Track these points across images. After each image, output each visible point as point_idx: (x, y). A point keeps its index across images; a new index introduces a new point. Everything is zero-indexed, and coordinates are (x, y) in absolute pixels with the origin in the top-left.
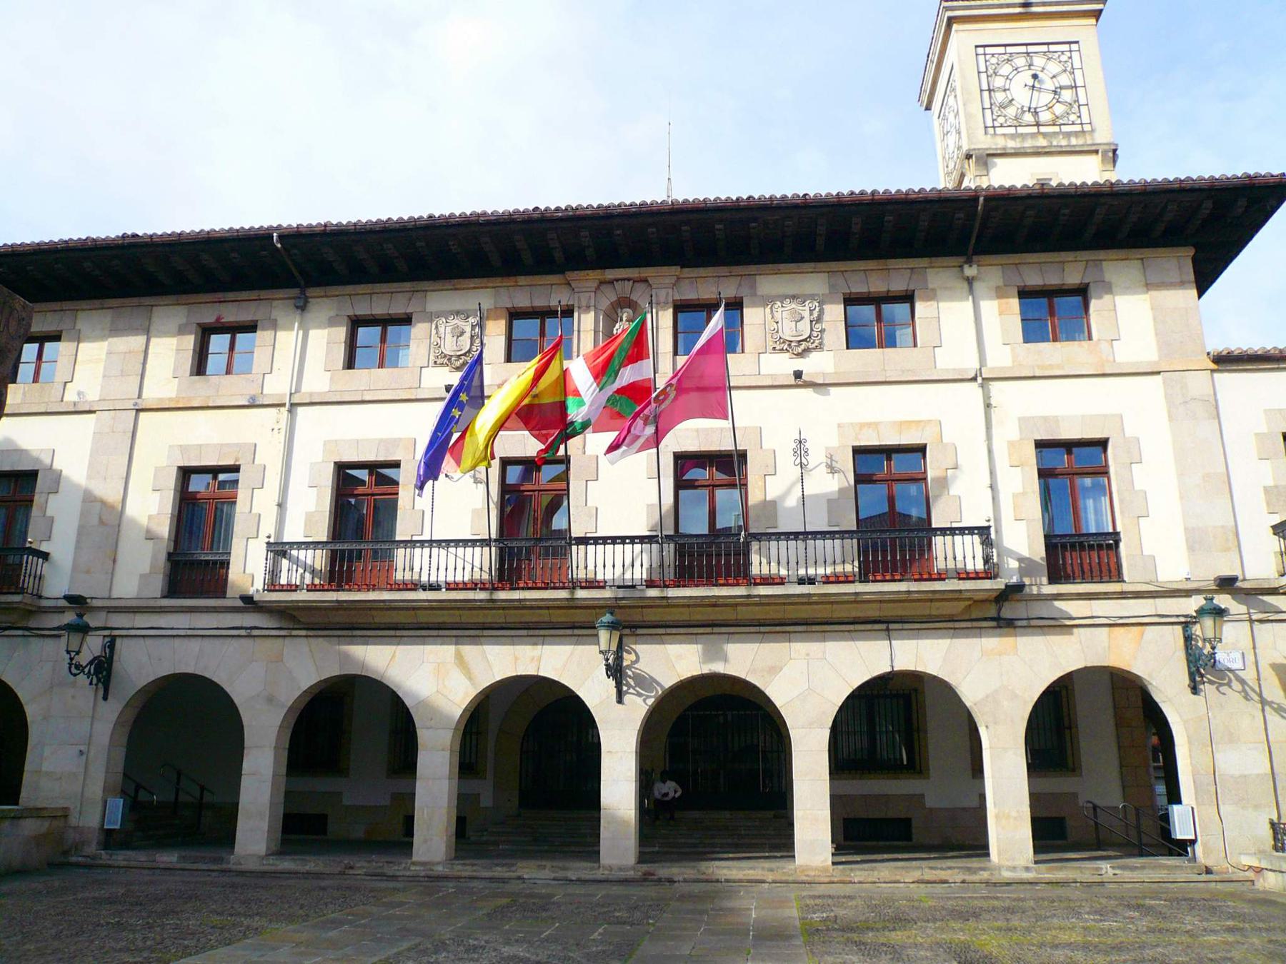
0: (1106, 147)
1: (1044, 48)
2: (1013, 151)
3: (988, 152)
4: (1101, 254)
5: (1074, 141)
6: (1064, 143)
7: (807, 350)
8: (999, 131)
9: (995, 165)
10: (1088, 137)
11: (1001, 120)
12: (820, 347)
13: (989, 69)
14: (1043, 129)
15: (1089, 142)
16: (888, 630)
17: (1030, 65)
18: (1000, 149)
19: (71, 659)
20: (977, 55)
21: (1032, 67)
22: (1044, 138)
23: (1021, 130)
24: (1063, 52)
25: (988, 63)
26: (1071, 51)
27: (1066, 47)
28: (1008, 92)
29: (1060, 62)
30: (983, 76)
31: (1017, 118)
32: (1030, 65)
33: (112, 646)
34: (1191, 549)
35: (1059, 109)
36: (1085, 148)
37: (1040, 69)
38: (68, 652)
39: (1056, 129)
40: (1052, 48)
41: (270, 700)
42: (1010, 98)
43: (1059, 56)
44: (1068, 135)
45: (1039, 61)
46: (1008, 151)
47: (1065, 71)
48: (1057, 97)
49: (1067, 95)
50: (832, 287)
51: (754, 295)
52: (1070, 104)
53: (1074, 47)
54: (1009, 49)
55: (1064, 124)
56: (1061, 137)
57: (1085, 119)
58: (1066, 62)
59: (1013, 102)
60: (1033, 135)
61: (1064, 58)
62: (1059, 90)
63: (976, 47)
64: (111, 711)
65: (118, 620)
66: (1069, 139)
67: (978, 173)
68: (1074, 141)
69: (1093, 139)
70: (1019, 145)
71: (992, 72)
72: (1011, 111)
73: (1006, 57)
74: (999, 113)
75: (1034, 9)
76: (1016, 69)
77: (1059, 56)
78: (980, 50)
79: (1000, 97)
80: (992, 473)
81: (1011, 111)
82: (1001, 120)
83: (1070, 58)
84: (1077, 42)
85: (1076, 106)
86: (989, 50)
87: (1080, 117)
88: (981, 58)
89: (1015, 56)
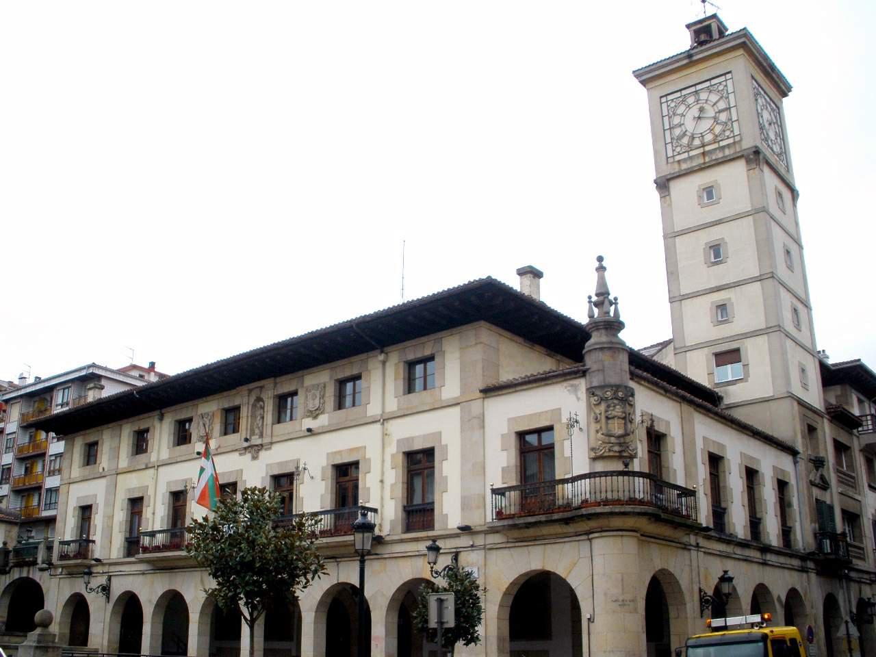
1: (707, 84)
4: (439, 335)
5: (727, 152)
6: (720, 155)
7: (317, 415)
10: (737, 146)
11: (678, 149)
12: (322, 413)
13: (670, 112)
14: (707, 148)
15: (738, 150)
16: (336, 561)
17: (697, 101)
18: (676, 173)
19: (432, 568)
20: (661, 103)
21: (700, 102)
23: (692, 153)
24: (720, 83)
26: (726, 80)
27: (722, 79)
28: (683, 127)
29: (718, 92)
32: (697, 101)
33: (109, 579)
34: (463, 509)
35: (718, 129)
37: (704, 101)
38: (429, 563)
39: (716, 146)
40: (714, 82)
41: (150, 601)
44: (723, 148)
45: (703, 96)
49: (723, 117)
50: (331, 377)
51: (303, 387)
52: (726, 123)
53: (729, 76)
54: (684, 92)
55: (722, 140)
57: (736, 132)
58: (722, 90)
63: (661, 97)
64: (110, 606)
65: (112, 569)
67: (663, 195)
69: (741, 147)
71: (672, 113)
72: (685, 141)
75: (695, 58)
78: (664, 100)
79: (677, 132)
80: (383, 473)
81: (685, 141)
82: (678, 149)
85: (729, 123)
86: (670, 98)
87: (732, 131)
88: (664, 106)
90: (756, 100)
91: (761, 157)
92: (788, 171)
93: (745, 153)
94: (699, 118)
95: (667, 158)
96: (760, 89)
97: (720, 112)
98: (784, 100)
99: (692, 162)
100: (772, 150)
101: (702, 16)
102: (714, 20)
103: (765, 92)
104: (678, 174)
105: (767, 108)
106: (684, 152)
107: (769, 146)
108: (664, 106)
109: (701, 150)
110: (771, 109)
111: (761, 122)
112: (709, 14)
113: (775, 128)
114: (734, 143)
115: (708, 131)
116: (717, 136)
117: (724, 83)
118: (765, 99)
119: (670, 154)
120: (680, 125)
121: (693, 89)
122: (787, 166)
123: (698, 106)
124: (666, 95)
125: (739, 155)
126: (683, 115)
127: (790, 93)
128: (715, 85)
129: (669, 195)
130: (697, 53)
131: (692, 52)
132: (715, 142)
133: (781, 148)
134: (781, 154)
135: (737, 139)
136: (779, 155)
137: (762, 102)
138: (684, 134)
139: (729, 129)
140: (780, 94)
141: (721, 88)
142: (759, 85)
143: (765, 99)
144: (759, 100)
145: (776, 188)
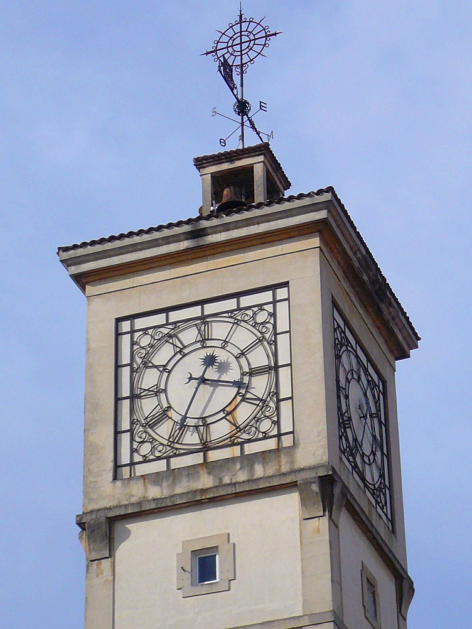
0: (311, 475)
1: (231, 304)
2: (153, 506)
3: (111, 514)
5: (259, 471)
6: (242, 477)
8: (141, 470)
9: (128, 533)
10: (284, 459)
11: (146, 449)
14: (214, 456)
18: (132, 504)
21: (209, 343)
22: (209, 473)
23: (177, 463)
24: (260, 307)
25: (136, 347)
26: (274, 302)
27: (267, 296)
30: (126, 372)
31: (173, 441)
36: (275, 482)
37: (219, 344)
39: (236, 451)
40: (245, 301)
42: (165, 405)
43: (255, 314)
46: (146, 507)
47: (260, 341)
48: (243, 391)
53: (282, 293)
54: (175, 316)
55: (249, 441)
56: (238, 466)
57: (286, 426)
59: (169, 414)
60: (191, 470)
61: (262, 317)
62: (246, 379)
63: (119, 320)
66: (252, 469)
67: (95, 555)
68: (259, 471)
69: (292, 462)
70: (166, 493)
71: (139, 361)
73: (165, 331)
74: (144, 436)
76: (180, 352)
77: (255, 314)
82: (146, 449)
83: (273, 315)
84: (286, 284)
86: (140, 323)
87: (277, 423)
89: (182, 326)
90: (338, 357)
91: (337, 491)
92: (393, 531)
93: (300, 478)
94: (203, 380)
95: (117, 467)
96: (348, 334)
97: (253, 373)
98: (399, 364)
99: (174, 483)
100: (363, 479)
101: (234, 145)
102: (261, 158)
103: (358, 342)
104: (136, 510)
105: (359, 378)
106: (159, 458)
107: (355, 467)
108: (126, 340)
109: (198, 458)
110: (368, 381)
111: (344, 409)
112: (252, 141)
113: (373, 428)
114: (278, 450)
115: (222, 415)
116: (239, 429)
117: (270, 308)
118: (357, 357)
119: (125, 458)
120: (157, 392)
121: (195, 312)
122: (392, 521)
123: (203, 353)
124: (132, 317)
125: (288, 480)
126: (164, 369)
127: (412, 352)
128: (249, 308)
129: (111, 555)
130: (216, 230)
131: (205, 224)
132: (233, 444)
133: (382, 476)
134: (380, 489)
135: (287, 441)
136: (377, 492)
137: (351, 364)
138: (164, 414)
139: (268, 417)
140: (391, 351)
141: (262, 317)
142: (347, 323)
143: (357, 357)
144: (344, 358)
145: (363, 569)
